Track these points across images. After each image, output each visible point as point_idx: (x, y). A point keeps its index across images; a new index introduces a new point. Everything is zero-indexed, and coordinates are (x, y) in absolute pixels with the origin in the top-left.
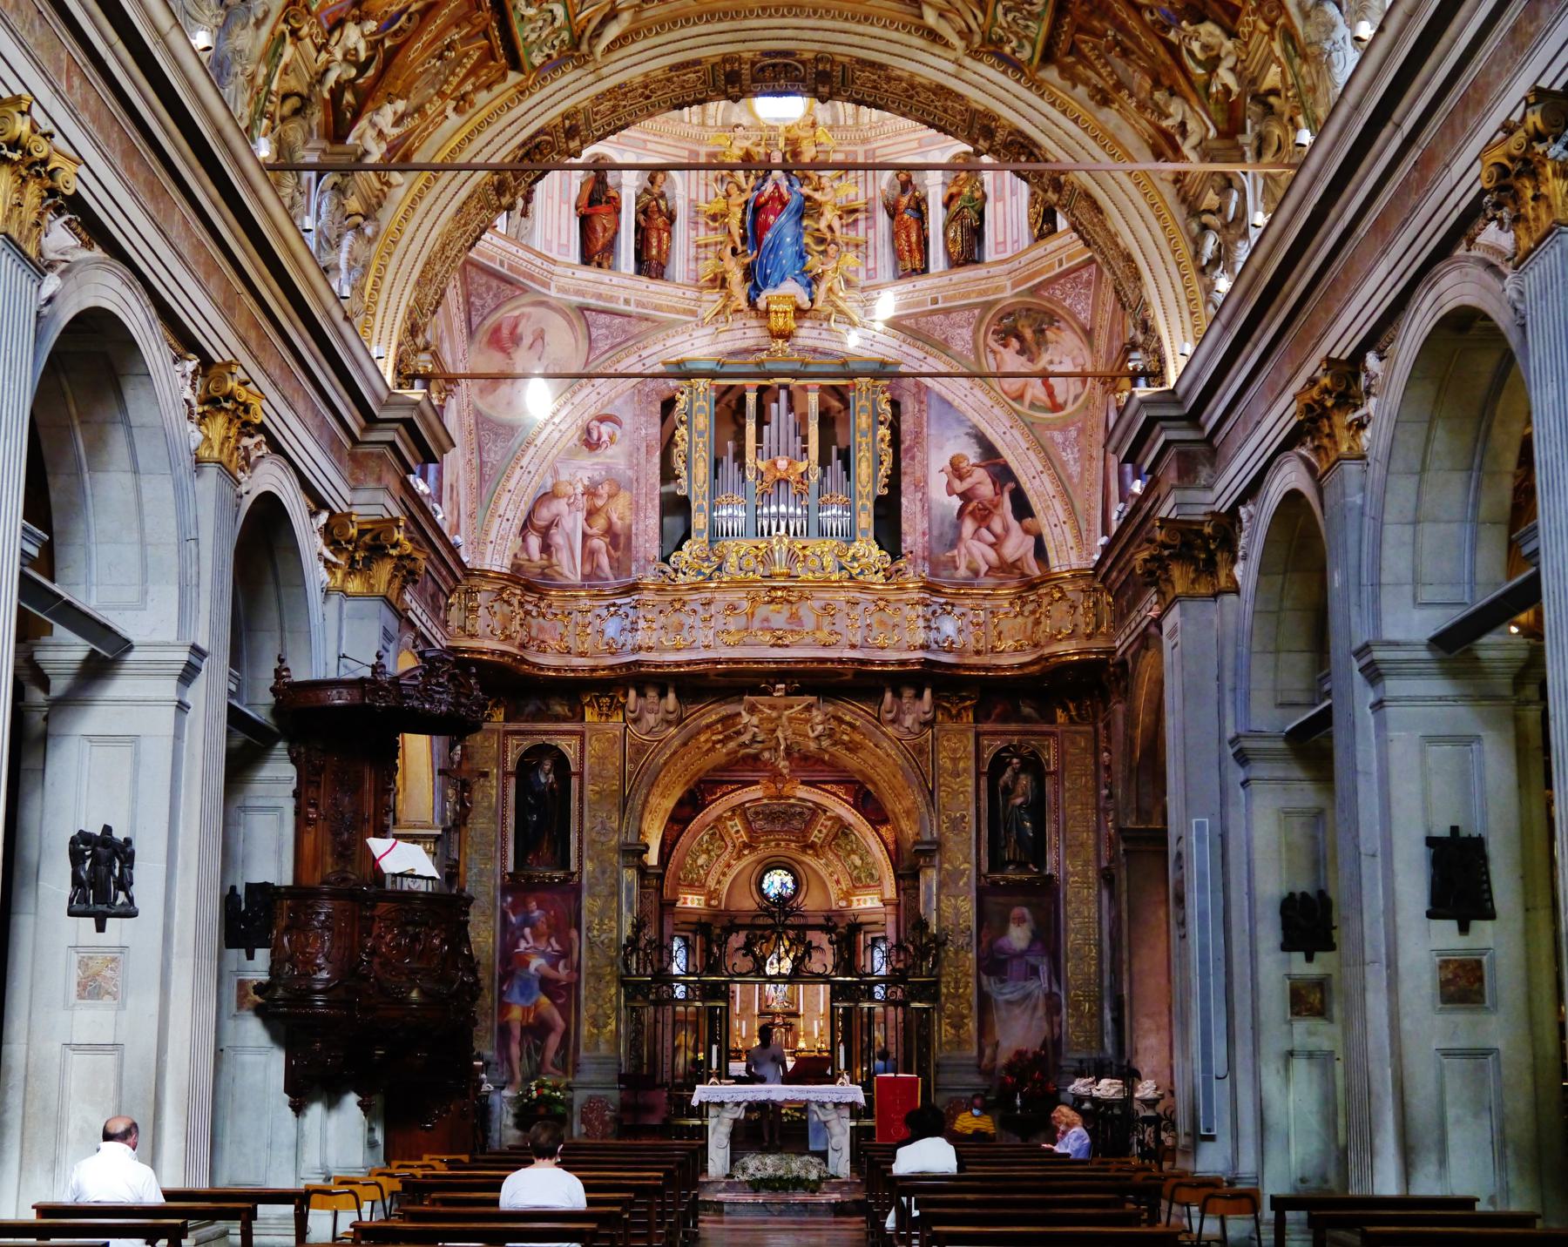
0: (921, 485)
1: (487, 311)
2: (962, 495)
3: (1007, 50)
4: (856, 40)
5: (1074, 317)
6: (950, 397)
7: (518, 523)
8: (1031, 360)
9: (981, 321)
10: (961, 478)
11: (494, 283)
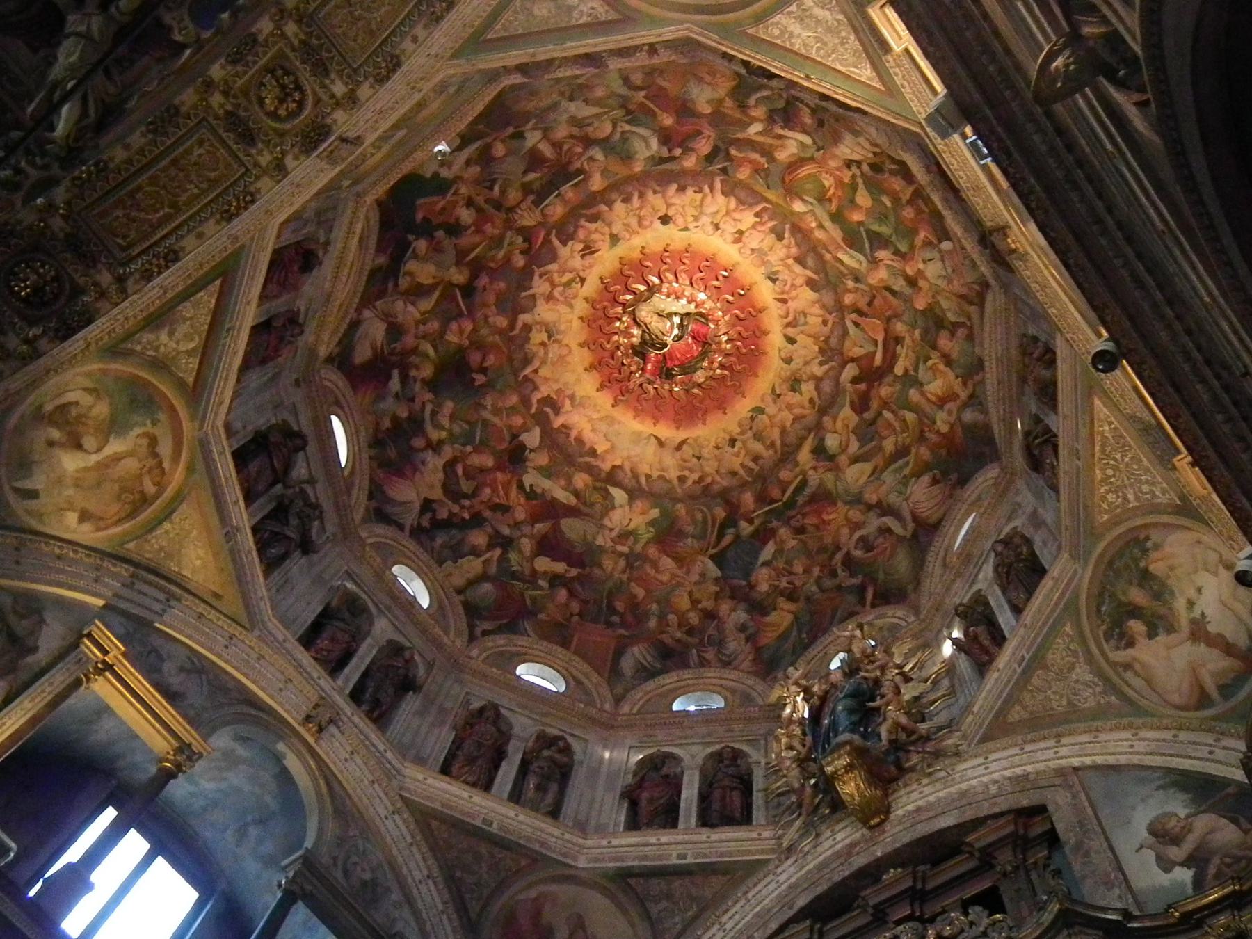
1: (486, 892)
2: (1187, 863)
5: (1154, 509)
6: (1111, 760)
8: (1171, 629)
9: (1084, 641)
10: (1176, 841)
11: (484, 849)
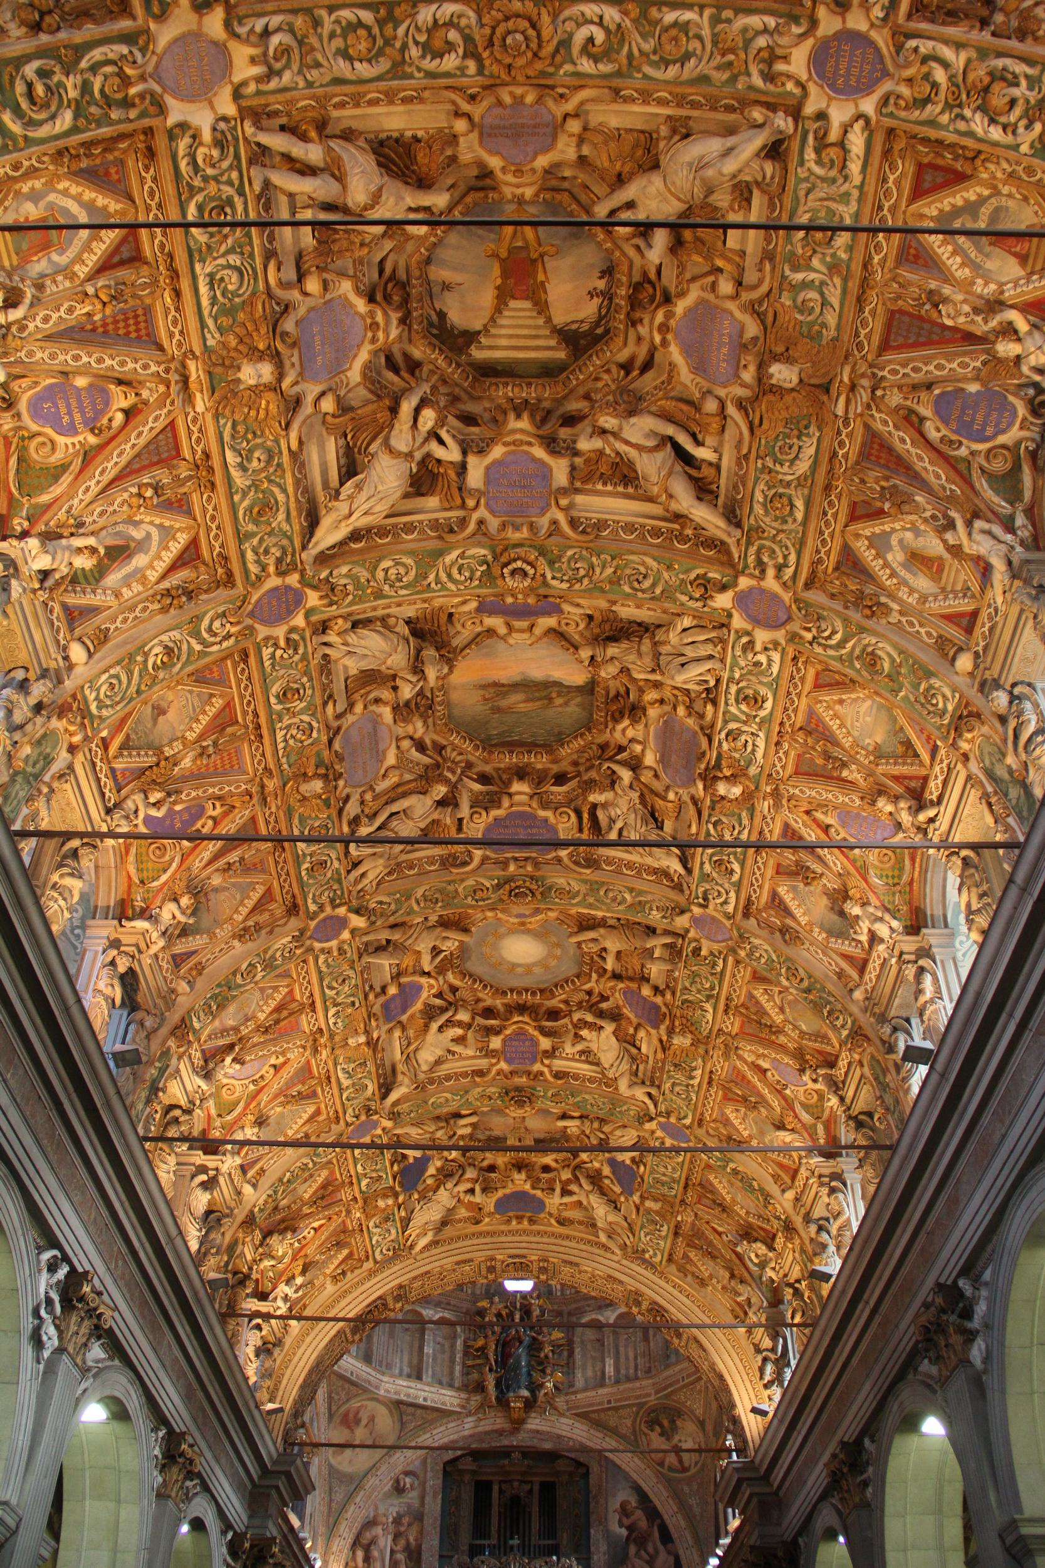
0: (603, 1521)
2: (628, 1528)
3: (647, 1256)
4: (562, 1249)
5: (692, 1412)
6: (619, 1462)
7: (350, 1541)
8: (668, 1439)
10: (627, 1516)
11: (347, 1386)
